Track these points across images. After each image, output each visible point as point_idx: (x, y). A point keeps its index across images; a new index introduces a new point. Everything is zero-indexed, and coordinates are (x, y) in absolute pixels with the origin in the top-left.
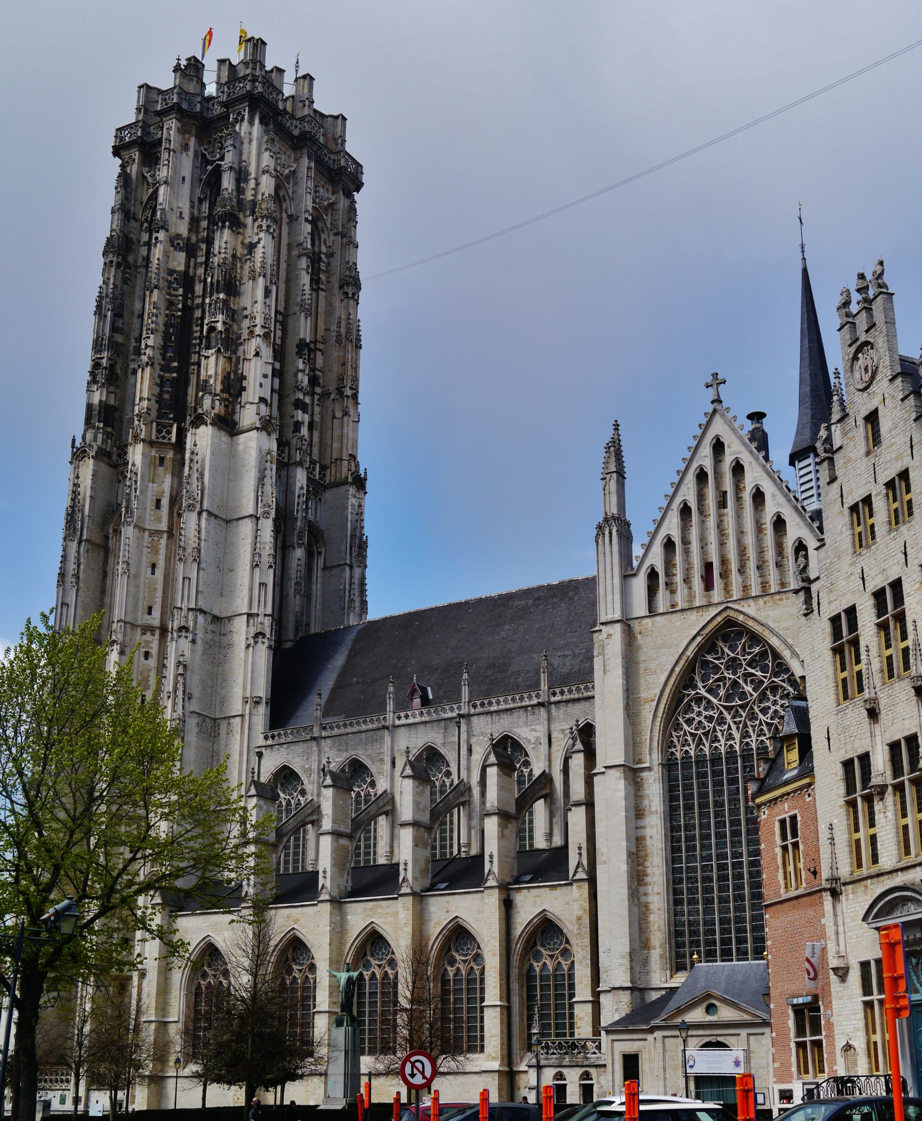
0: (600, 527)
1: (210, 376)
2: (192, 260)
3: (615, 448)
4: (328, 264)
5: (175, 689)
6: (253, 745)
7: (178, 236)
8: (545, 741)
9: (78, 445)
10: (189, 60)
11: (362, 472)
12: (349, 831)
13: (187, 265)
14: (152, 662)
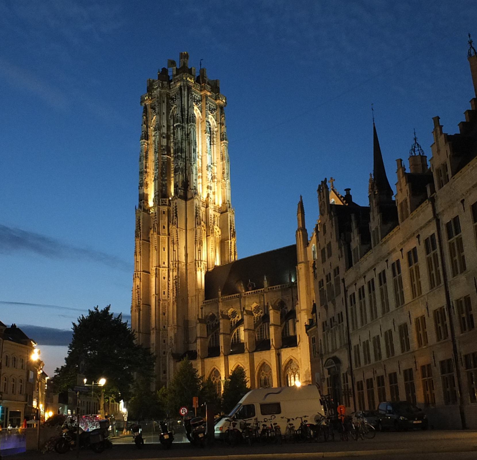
0: (297, 232)
1: (177, 182)
3: (301, 205)
4: (217, 135)
5: (173, 288)
6: (200, 305)
7: (163, 133)
8: (291, 299)
10: (162, 69)
12: (229, 333)
13: (167, 143)
14: (166, 279)
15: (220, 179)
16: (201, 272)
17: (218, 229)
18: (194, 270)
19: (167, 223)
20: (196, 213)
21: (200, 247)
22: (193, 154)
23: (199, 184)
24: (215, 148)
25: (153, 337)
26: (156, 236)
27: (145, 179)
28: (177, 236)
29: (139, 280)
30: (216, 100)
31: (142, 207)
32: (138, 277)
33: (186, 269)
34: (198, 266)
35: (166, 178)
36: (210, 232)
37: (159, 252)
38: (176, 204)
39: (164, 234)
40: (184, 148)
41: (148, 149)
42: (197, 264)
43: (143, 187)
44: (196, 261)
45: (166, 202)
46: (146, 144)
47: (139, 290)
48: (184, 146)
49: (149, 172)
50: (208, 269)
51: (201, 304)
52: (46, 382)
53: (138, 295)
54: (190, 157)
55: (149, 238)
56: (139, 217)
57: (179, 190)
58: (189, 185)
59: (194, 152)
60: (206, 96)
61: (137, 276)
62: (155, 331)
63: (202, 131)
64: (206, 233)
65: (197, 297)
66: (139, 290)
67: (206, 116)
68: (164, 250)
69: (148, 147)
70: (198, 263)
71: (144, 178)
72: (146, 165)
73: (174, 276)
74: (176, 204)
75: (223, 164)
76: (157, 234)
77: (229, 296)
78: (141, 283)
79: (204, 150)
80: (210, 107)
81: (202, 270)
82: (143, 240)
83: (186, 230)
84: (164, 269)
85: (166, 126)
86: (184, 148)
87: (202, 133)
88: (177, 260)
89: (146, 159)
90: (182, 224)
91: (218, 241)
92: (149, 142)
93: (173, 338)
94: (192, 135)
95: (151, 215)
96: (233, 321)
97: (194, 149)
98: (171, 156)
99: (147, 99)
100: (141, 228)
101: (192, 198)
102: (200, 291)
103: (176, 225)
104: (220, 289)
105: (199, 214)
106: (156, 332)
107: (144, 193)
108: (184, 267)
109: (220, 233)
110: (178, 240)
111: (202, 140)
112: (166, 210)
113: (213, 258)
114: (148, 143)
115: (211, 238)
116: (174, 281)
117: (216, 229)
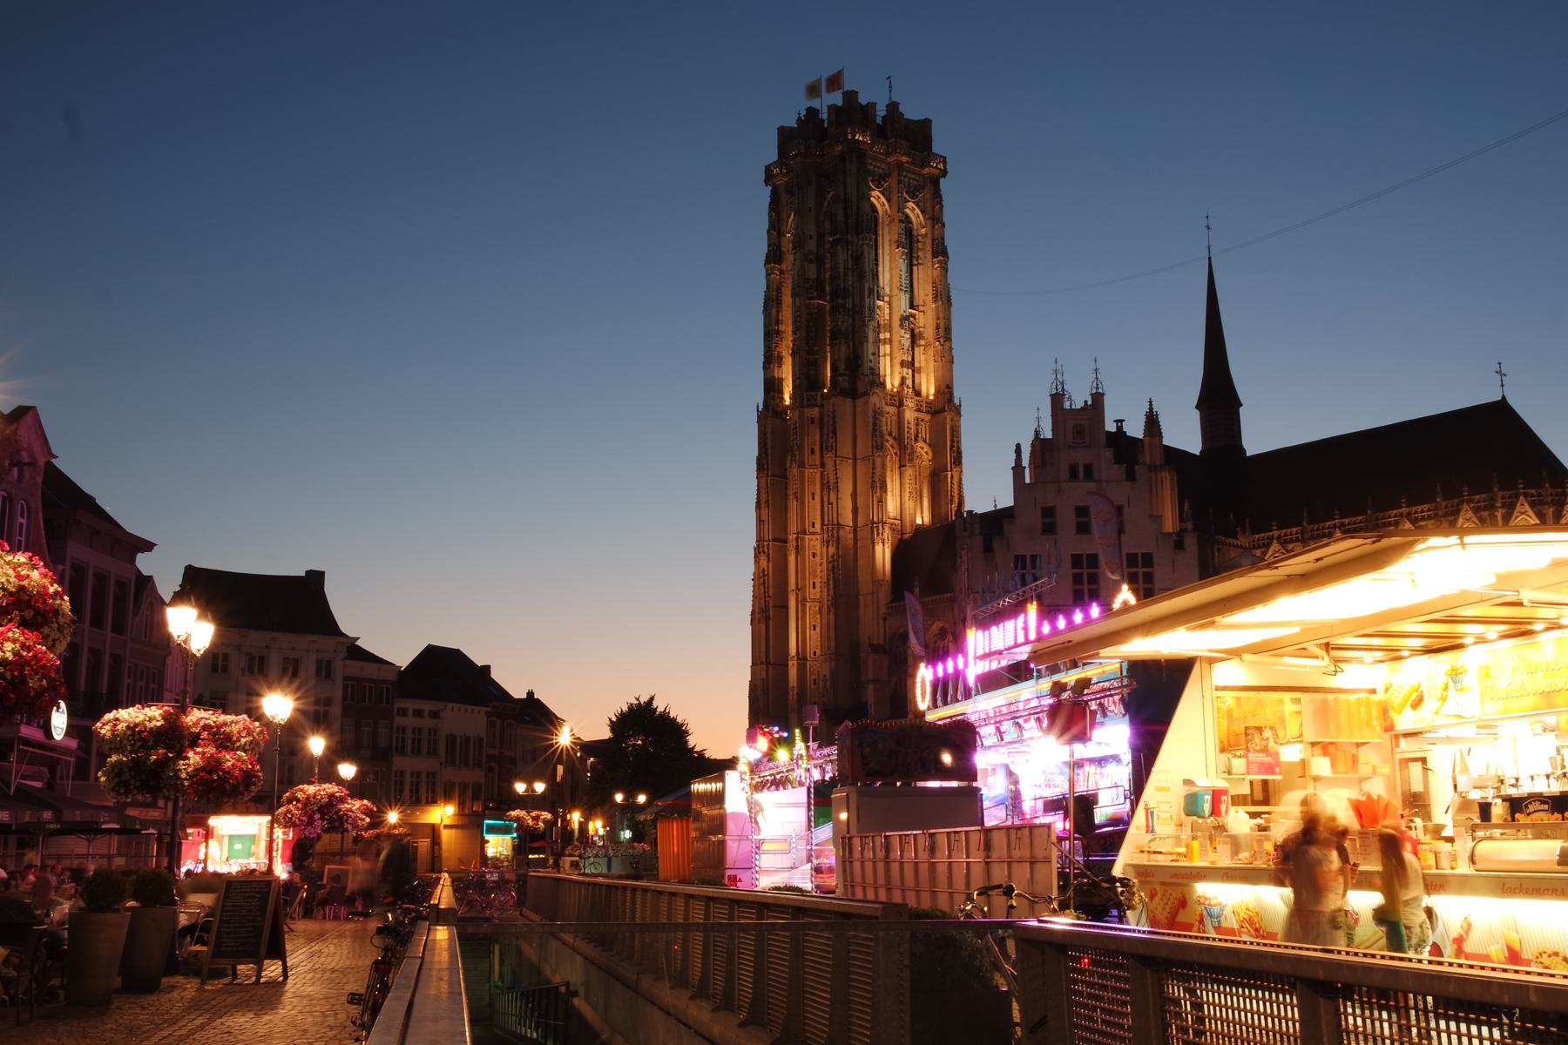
2: (822, 268)
4: (925, 242)
5: (828, 580)
9: (760, 410)
11: (956, 401)
13: (819, 273)
15: (932, 341)
16: (884, 545)
17: (926, 448)
18: (869, 541)
19: (818, 443)
20: (875, 424)
21: (881, 495)
22: (867, 300)
23: (885, 355)
24: (921, 272)
25: (793, 672)
26: (795, 471)
27: (776, 347)
28: (836, 474)
29: (766, 559)
30: (923, 167)
31: (770, 407)
32: (764, 552)
33: (855, 540)
34: (878, 535)
35: (816, 348)
36: (907, 457)
37: (803, 503)
38: (834, 405)
39: (813, 466)
40: (850, 288)
41: (781, 283)
42: (875, 529)
43: (772, 366)
44: (873, 523)
45: (815, 400)
46: (778, 273)
47: (766, 578)
48: (850, 283)
49: (782, 332)
50: (902, 534)
51: (883, 610)
52: (589, 768)
53: (765, 588)
54: (863, 307)
55: (786, 470)
56: (765, 428)
57: (840, 378)
58: (859, 366)
59: (869, 297)
60: (900, 166)
61: (761, 550)
62: (795, 662)
63: (890, 241)
64: (897, 459)
65: (875, 596)
66: (766, 578)
67: (899, 208)
68: (813, 498)
69: (781, 278)
70: (878, 527)
71: (774, 345)
72: (778, 316)
73: (831, 553)
74: (834, 405)
75: (937, 308)
76: (799, 467)
77: (934, 598)
78: (770, 564)
79: (896, 283)
80: (909, 183)
81: (886, 541)
82: (773, 476)
83: (855, 459)
84: (814, 537)
85: (814, 237)
86: (850, 288)
87: (890, 245)
88: (835, 522)
89: (777, 303)
90: (845, 449)
91: (927, 473)
92: (784, 267)
93: (828, 676)
94: (866, 260)
95: (789, 423)
96: (941, 646)
97: (869, 288)
98: (825, 301)
99: (777, 174)
100: (769, 451)
101: (866, 394)
102: (881, 585)
103: (834, 452)
104: (916, 583)
105: (880, 426)
106: (798, 664)
107: (774, 377)
108: (851, 536)
109: (930, 457)
110: (837, 482)
111: (891, 262)
112: (817, 415)
113: (912, 511)
114: (782, 272)
115: (909, 472)
116: (830, 566)
117: (922, 448)
